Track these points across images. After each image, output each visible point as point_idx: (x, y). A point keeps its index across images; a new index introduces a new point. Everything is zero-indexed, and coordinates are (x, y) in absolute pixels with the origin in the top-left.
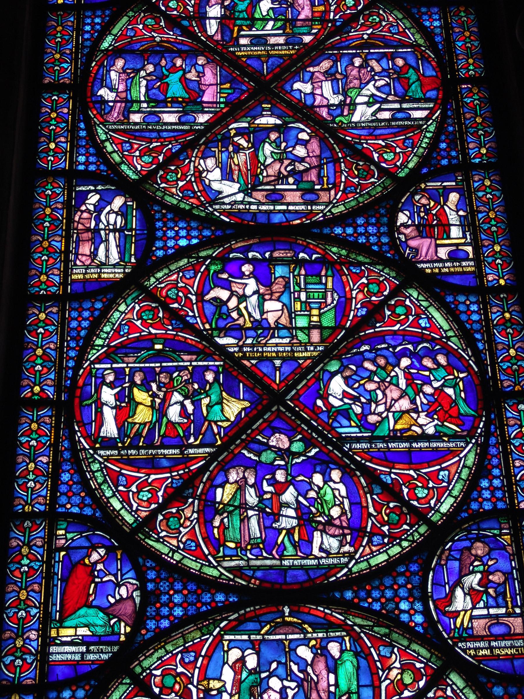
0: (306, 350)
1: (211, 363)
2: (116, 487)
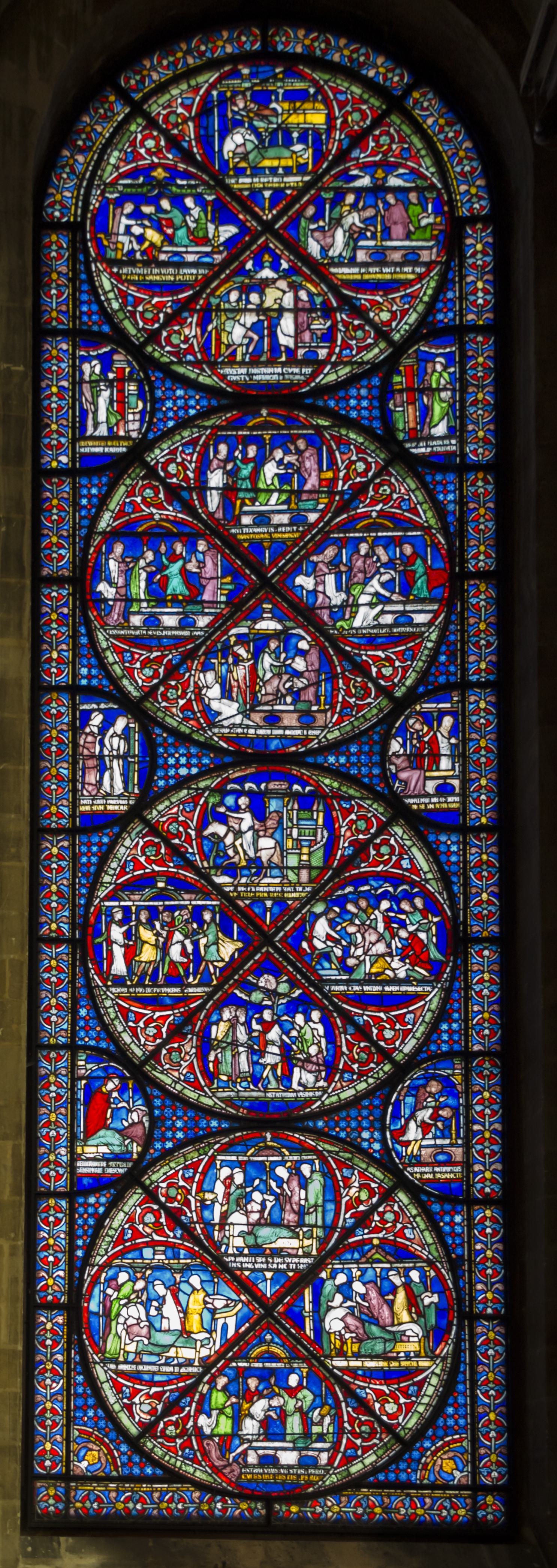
0: (295, 891)
1: (209, 903)
2: (127, 1021)
